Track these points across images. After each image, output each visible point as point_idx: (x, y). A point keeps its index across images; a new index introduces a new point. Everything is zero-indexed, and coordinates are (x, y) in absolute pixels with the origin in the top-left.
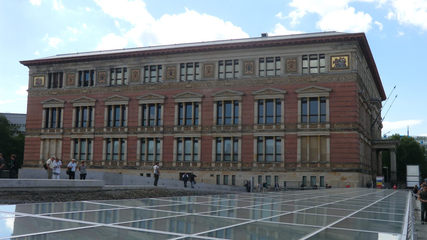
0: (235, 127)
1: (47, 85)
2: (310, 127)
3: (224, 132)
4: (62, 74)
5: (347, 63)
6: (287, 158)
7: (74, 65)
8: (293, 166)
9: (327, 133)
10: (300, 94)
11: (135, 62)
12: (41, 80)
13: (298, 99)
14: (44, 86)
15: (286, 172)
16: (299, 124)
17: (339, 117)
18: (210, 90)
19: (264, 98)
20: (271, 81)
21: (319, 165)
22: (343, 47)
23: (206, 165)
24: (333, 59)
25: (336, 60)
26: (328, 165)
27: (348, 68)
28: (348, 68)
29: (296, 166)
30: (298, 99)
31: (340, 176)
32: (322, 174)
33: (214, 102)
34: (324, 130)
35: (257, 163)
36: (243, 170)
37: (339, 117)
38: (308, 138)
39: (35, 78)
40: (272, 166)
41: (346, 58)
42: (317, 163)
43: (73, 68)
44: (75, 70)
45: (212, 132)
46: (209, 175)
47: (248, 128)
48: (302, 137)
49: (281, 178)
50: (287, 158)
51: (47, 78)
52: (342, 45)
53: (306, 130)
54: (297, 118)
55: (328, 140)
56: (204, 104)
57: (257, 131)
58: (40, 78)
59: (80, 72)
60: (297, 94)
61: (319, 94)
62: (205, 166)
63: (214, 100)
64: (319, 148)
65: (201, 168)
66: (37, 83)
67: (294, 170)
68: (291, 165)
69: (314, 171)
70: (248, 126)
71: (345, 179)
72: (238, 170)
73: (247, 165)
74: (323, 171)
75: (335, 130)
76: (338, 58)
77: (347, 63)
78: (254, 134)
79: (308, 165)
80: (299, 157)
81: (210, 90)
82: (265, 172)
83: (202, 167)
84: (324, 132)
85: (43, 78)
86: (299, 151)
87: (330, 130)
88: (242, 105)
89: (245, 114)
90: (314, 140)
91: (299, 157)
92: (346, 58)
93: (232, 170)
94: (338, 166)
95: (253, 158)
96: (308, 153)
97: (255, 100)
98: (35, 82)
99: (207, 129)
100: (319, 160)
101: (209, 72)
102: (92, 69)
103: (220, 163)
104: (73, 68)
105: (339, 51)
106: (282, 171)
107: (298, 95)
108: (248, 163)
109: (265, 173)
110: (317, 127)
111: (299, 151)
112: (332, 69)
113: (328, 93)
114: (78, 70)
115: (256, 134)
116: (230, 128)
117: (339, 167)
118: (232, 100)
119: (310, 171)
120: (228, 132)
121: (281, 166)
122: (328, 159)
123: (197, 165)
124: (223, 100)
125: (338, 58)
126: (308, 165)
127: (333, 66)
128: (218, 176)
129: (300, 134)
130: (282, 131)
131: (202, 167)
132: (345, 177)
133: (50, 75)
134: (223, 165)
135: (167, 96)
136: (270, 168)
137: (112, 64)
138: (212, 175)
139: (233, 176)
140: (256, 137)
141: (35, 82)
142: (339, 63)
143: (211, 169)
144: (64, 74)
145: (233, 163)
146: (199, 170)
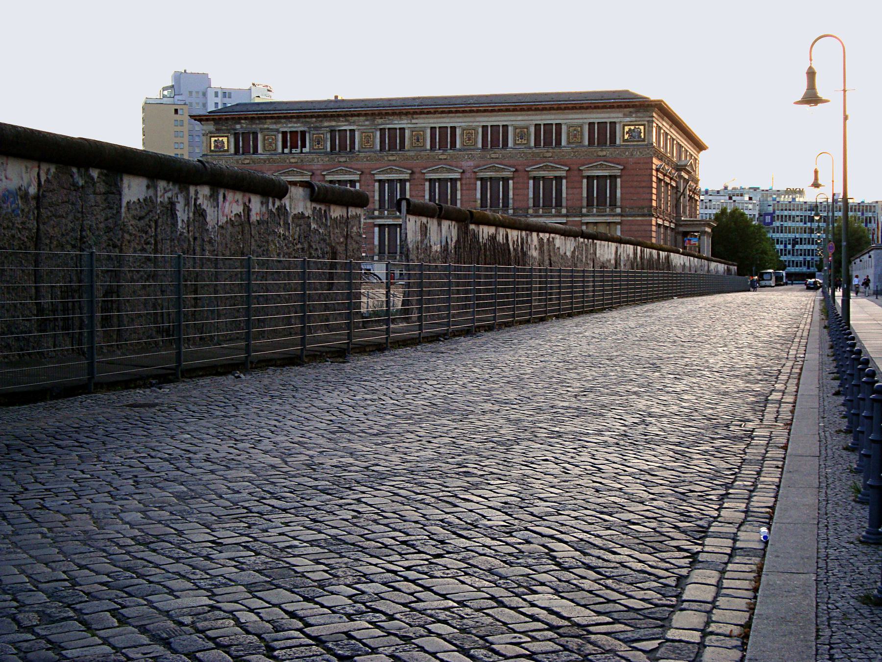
1: (232, 151)
4: (255, 135)
5: (642, 135)
7: (275, 123)
9: (618, 219)
11: (367, 123)
12: (223, 142)
13: (584, 177)
14: (227, 151)
18: (472, 163)
20: (550, 154)
22: (639, 115)
24: (627, 129)
25: (630, 129)
27: (644, 140)
28: (644, 140)
30: (584, 177)
33: (477, 179)
34: (614, 216)
39: (213, 139)
41: (642, 127)
43: (274, 127)
44: (277, 131)
51: (232, 140)
52: (636, 112)
56: (464, 182)
58: (221, 139)
59: (284, 134)
60: (581, 170)
66: (216, 146)
75: (628, 216)
76: (632, 128)
77: (642, 135)
81: (472, 163)
85: (225, 139)
92: (642, 127)
97: (530, 178)
98: (213, 145)
101: (469, 140)
102: (302, 129)
104: (274, 127)
105: (634, 119)
112: (624, 141)
114: (282, 130)
125: (632, 128)
127: (626, 137)
130: (564, 216)
133: (236, 136)
135: (415, 170)
137: (334, 124)
141: (213, 145)
142: (634, 134)
144: (259, 136)
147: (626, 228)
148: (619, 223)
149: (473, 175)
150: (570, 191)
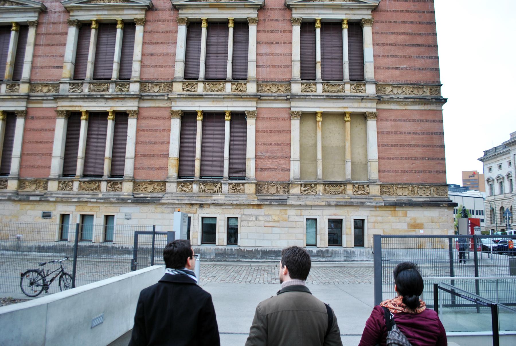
0: (123, 85)
2: (324, 91)
3: (89, 97)
6: (262, 170)
8: (278, 191)
9: (370, 107)
10: (298, 11)
15: (259, 206)
16: (296, 82)
17: (397, 68)
19: (204, 17)
21: (349, 189)
23: (34, 187)
26: (375, 190)
29: (288, 192)
30: (293, 21)
31: (408, 219)
32: (360, 214)
33: (70, 23)
35: (179, 183)
36: (138, 201)
37: (397, 68)
38: (319, 118)
40: (220, 191)
42: (344, 184)
45: (56, 98)
46: (40, 213)
47: (156, 89)
48: (304, 116)
49: (245, 223)
50: (262, 170)
53: (317, 98)
54: (290, 67)
55: (372, 124)
56: (43, 29)
57: (180, 98)
61: (348, 12)
62: (30, 189)
63: (72, 18)
64: (348, 144)
65: (17, 193)
67: (282, 203)
68: (273, 190)
69: (337, 205)
70: (158, 84)
71: (419, 226)
72: (123, 201)
73: (150, 188)
74: (362, 205)
78: (173, 104)
79: (320, 188)
80: (295, 168)
82: (201, 206)
83: (21, 192)
84: (363, 105)
86: (295, 152)
87: (379, 100)
88: (145, 32)
89: (152, 55)
90: (333, 126)
91: (295, 168)
93: (106, 201)
94: (400, 192)
95: (166, 169)
96: (319, 156)
97: (180, 21)
99: (45, 89)
100: (349, 177)
103: (72, 181)
106: (249, 205)
107: (294, 11)
108: (152, 182)
109: (199, 210)
110: (343, 90)
111: (295, 152)
113: (370, 12)
115: (179, 103)
116: (107, 89)
117: (403, 194)
118: (119, 18)
119: (329, 205)
120: (102, 97)
121: (246, 191)
122: (374, 174)
123: (6, 187)
124: (94, 18)
126: (320, 188)
128: (64, 217)
129: (299, 106)
131: (21, 192)
132: (418, 221)
134: (80, 186)
136: (215, 197)
138: (46, 215)
139: (108, 218)
140: (177, 112)
143: (43, 199)
145: (108, 182)
146: (10, 200)
147: (388, 126)
148: (374, 115)
149: (63, 18)
150: (266, 49)
